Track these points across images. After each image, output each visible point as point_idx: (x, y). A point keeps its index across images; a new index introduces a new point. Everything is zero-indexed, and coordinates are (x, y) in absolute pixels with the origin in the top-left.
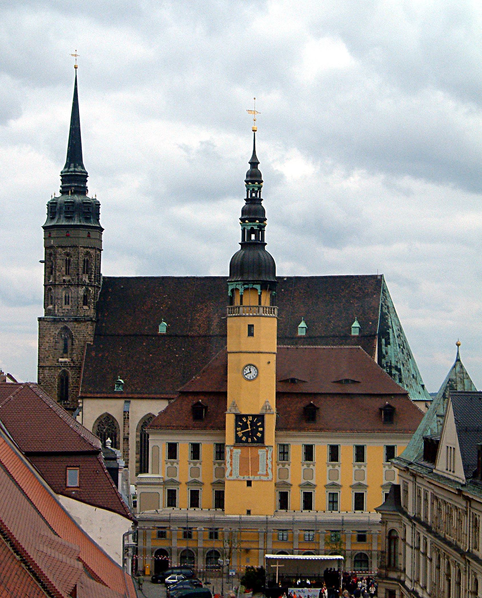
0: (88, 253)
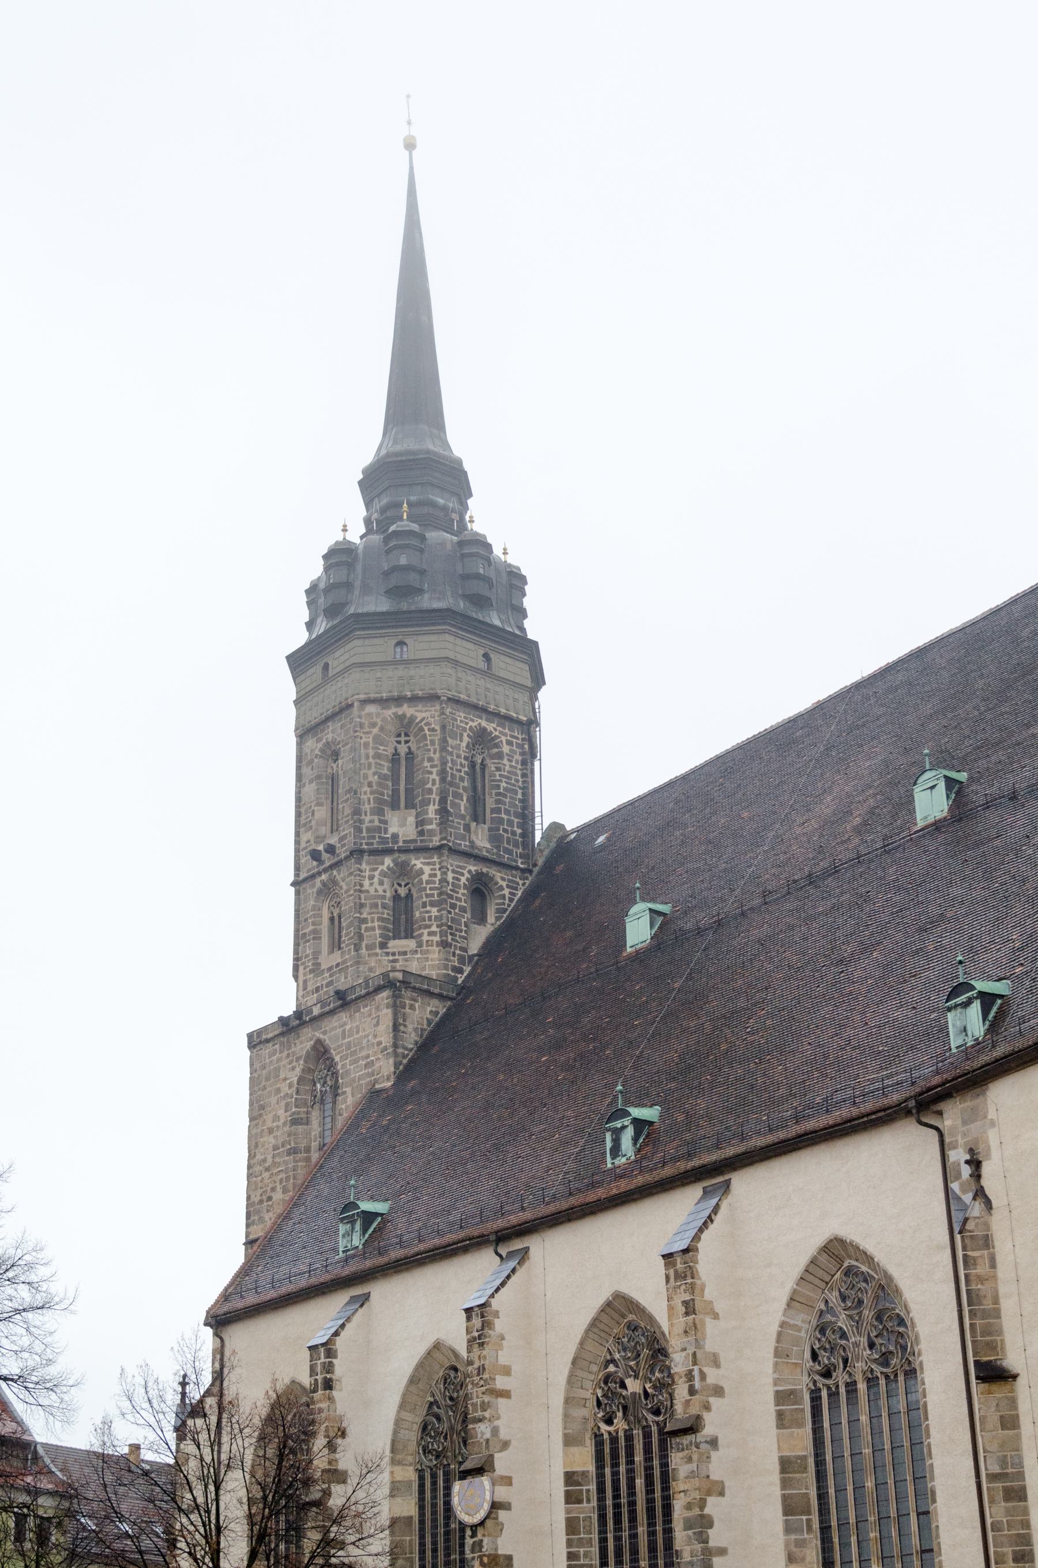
0: (406, 728)
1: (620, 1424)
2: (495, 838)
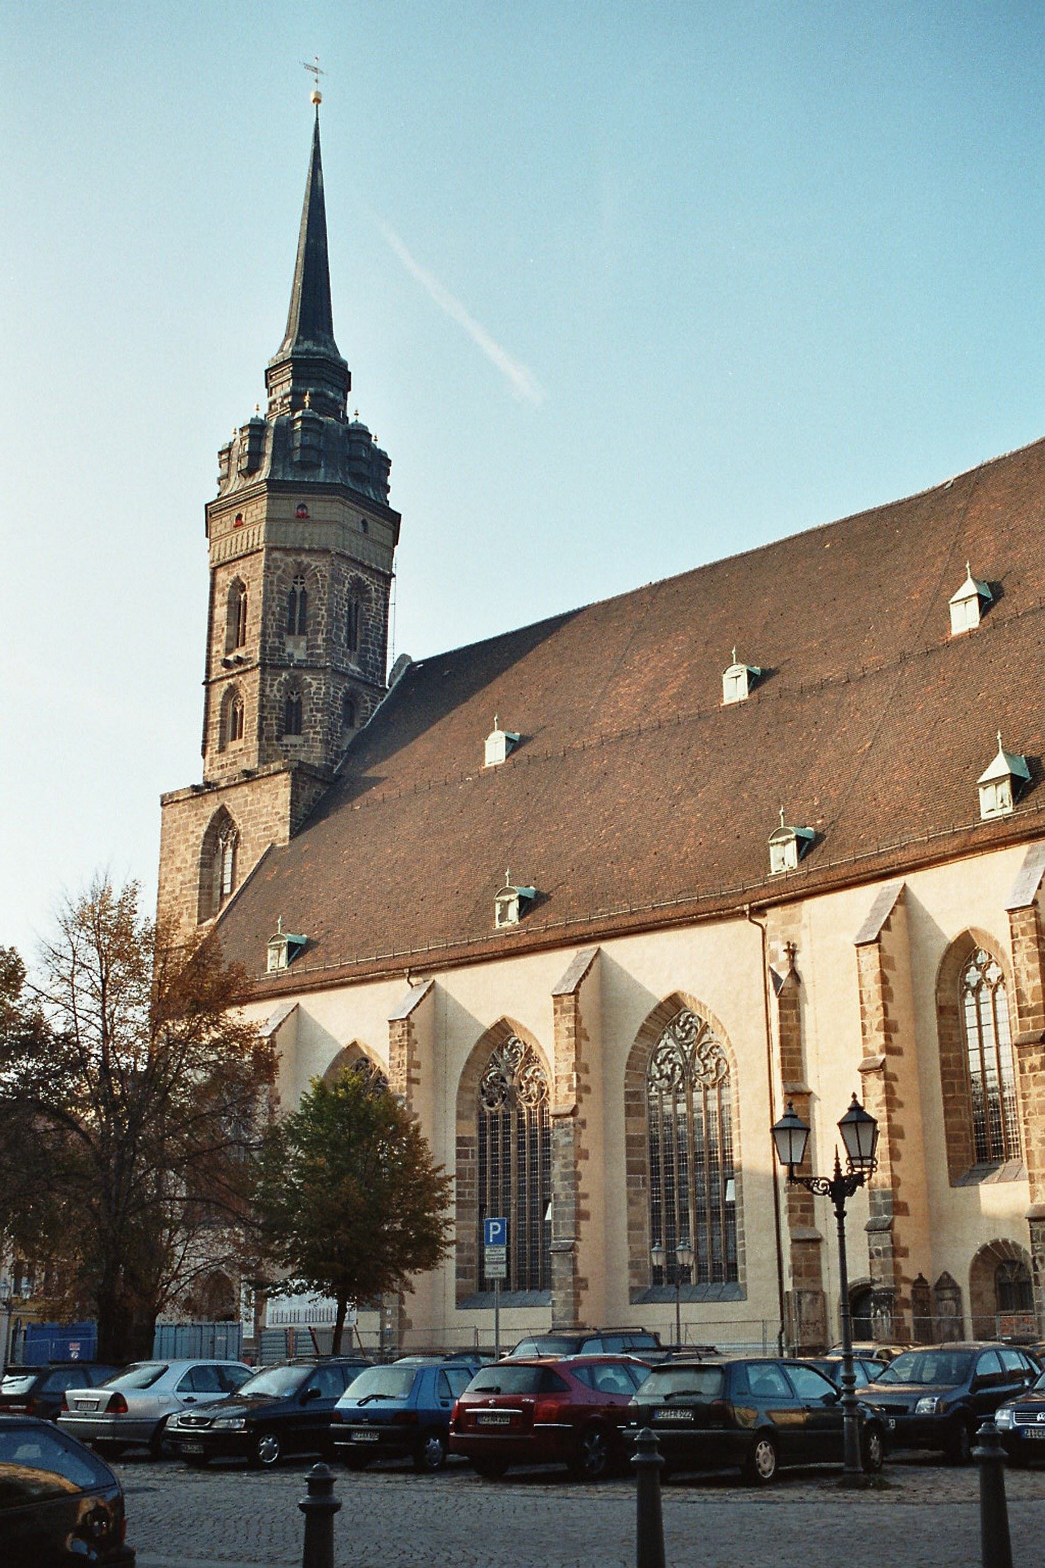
0: (301, 572)
1: (499, 1106)
2: (362, 663)
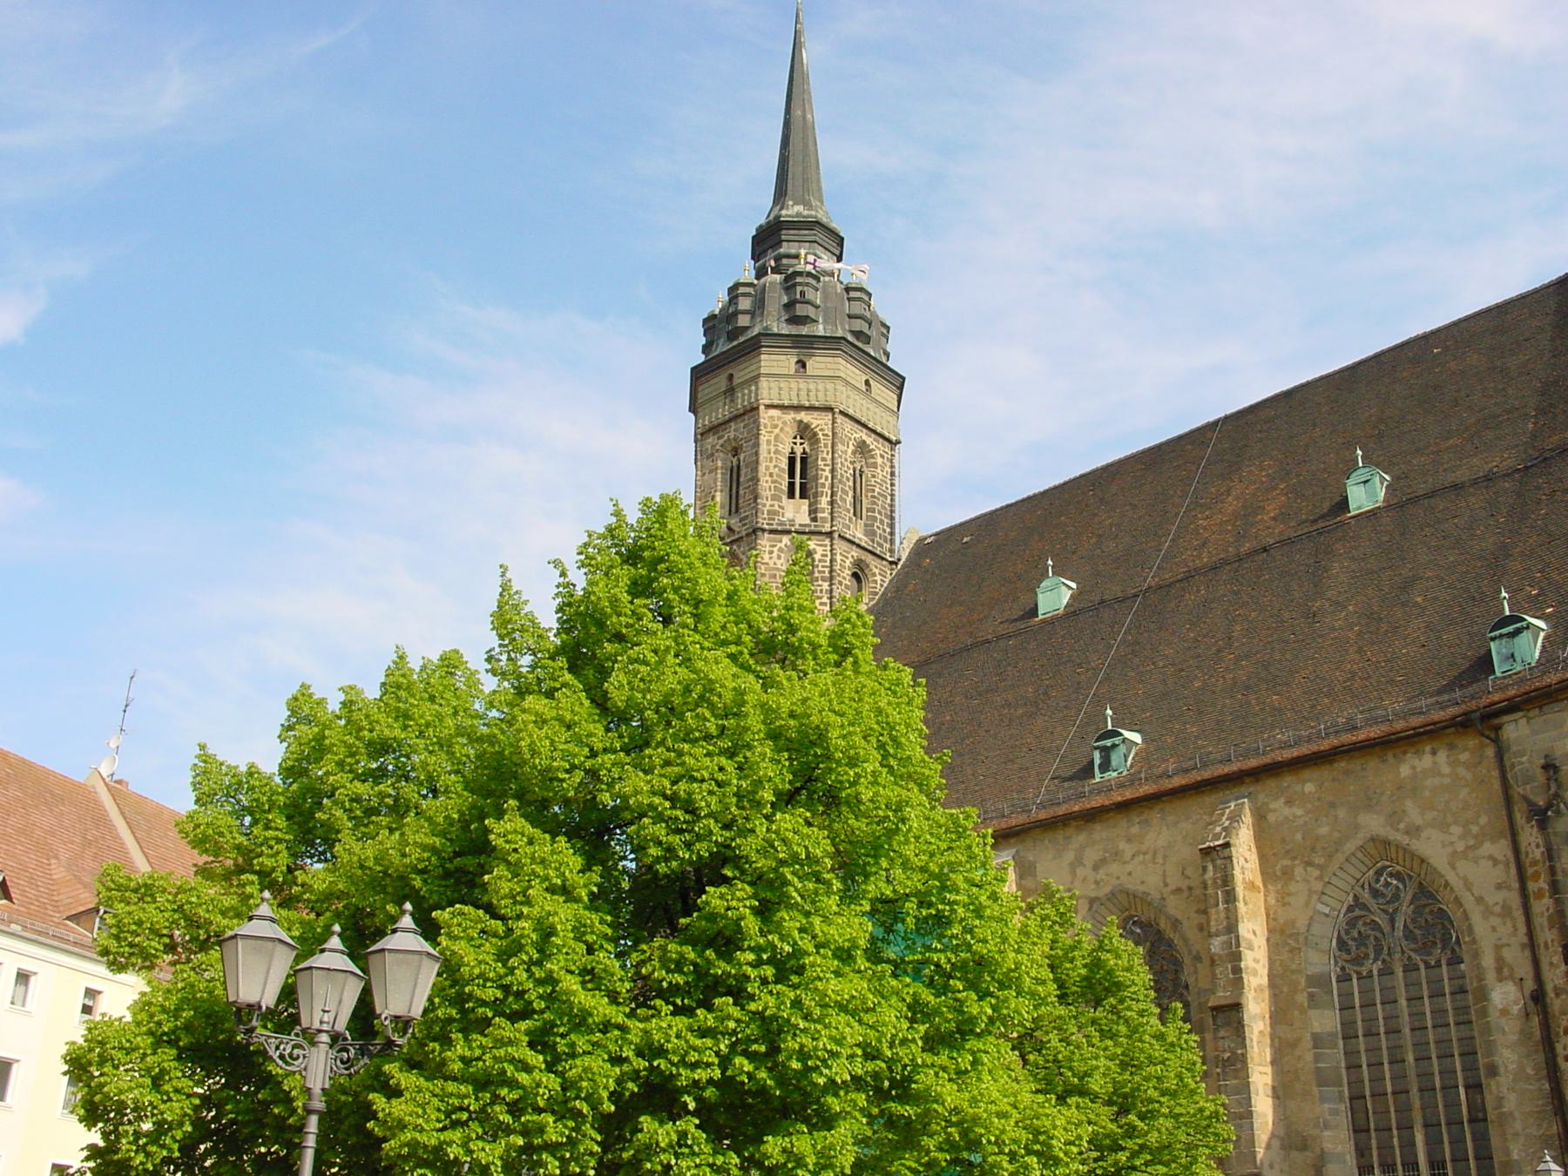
0: (804, 431)
2: (870, 533)
